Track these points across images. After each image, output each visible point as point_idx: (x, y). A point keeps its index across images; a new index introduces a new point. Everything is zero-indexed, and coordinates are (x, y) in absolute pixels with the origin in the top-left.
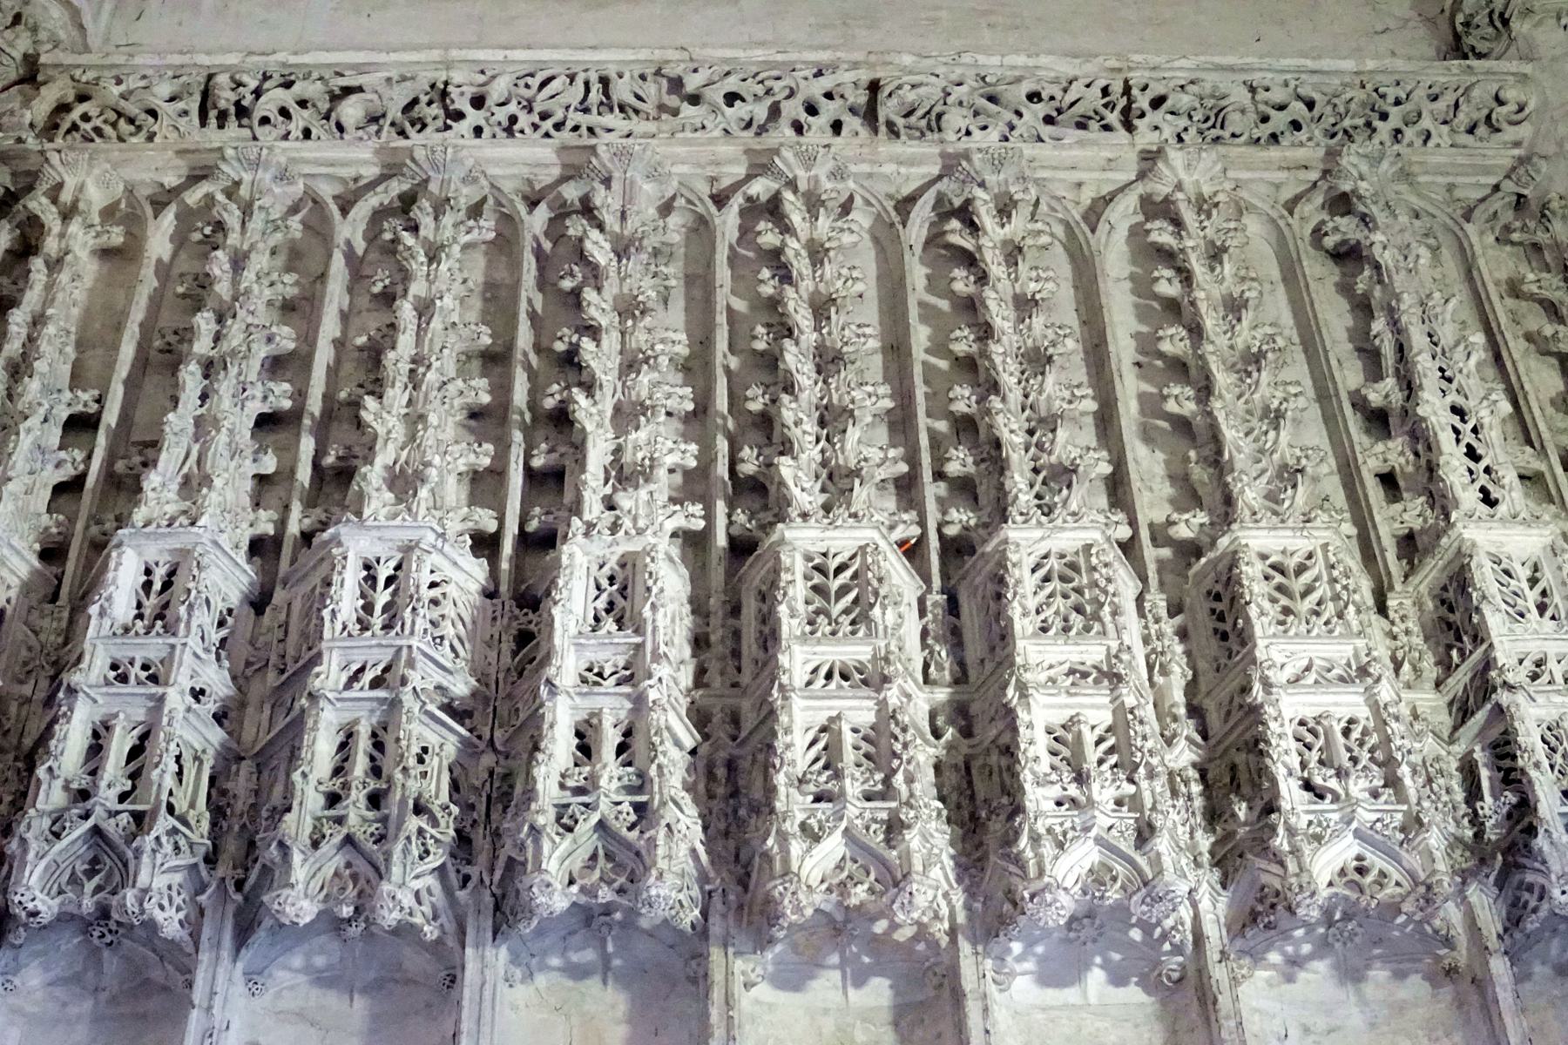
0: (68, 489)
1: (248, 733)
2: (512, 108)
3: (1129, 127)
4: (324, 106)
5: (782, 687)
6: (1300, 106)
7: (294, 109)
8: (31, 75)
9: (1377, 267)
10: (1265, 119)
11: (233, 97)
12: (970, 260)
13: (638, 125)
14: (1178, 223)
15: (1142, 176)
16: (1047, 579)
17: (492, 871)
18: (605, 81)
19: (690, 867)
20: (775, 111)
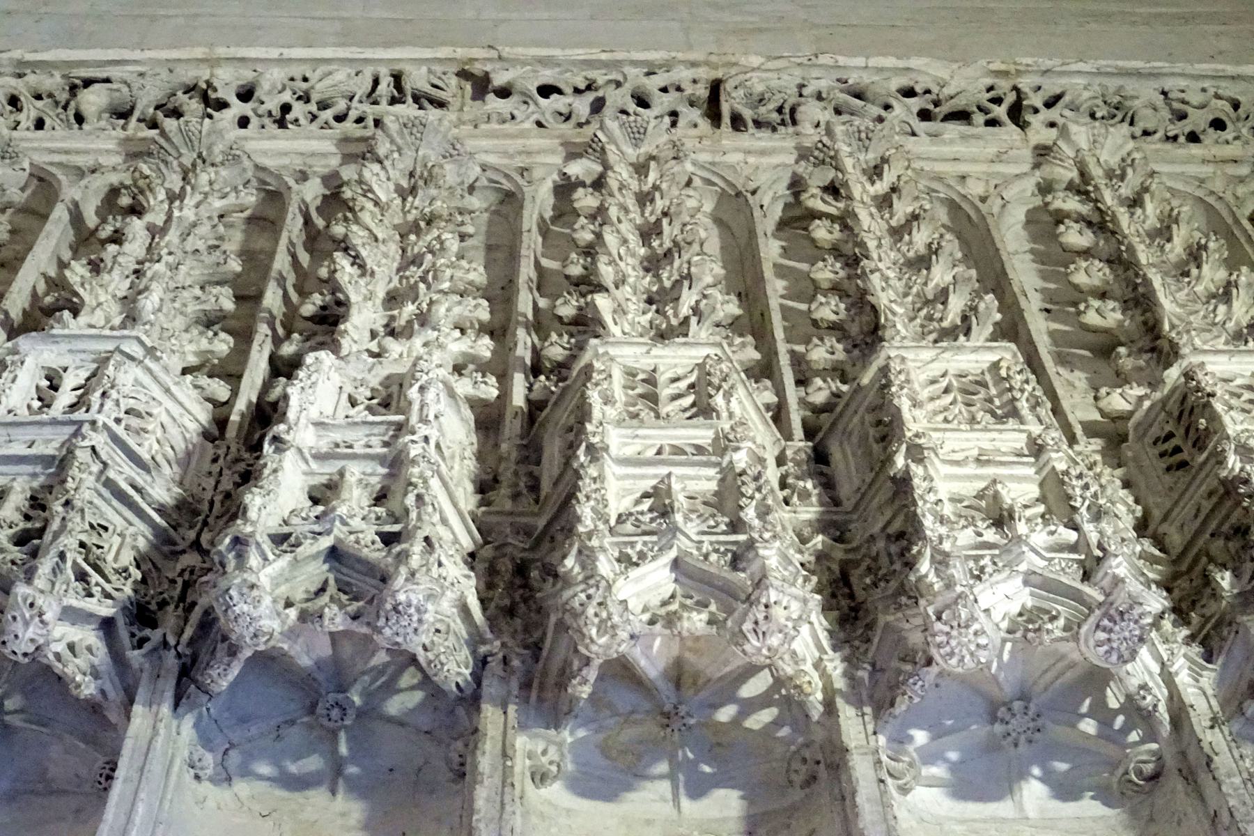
2: (287, 97)
3: (1023, 125)
4: (63, 97)
5: (591, 448)
7: (26, 99)
10: (1182, 116)
15: (1037, 166)
16: (947, 391)
17: (180, 633)
18: (397, 78)
19: (459, 627)
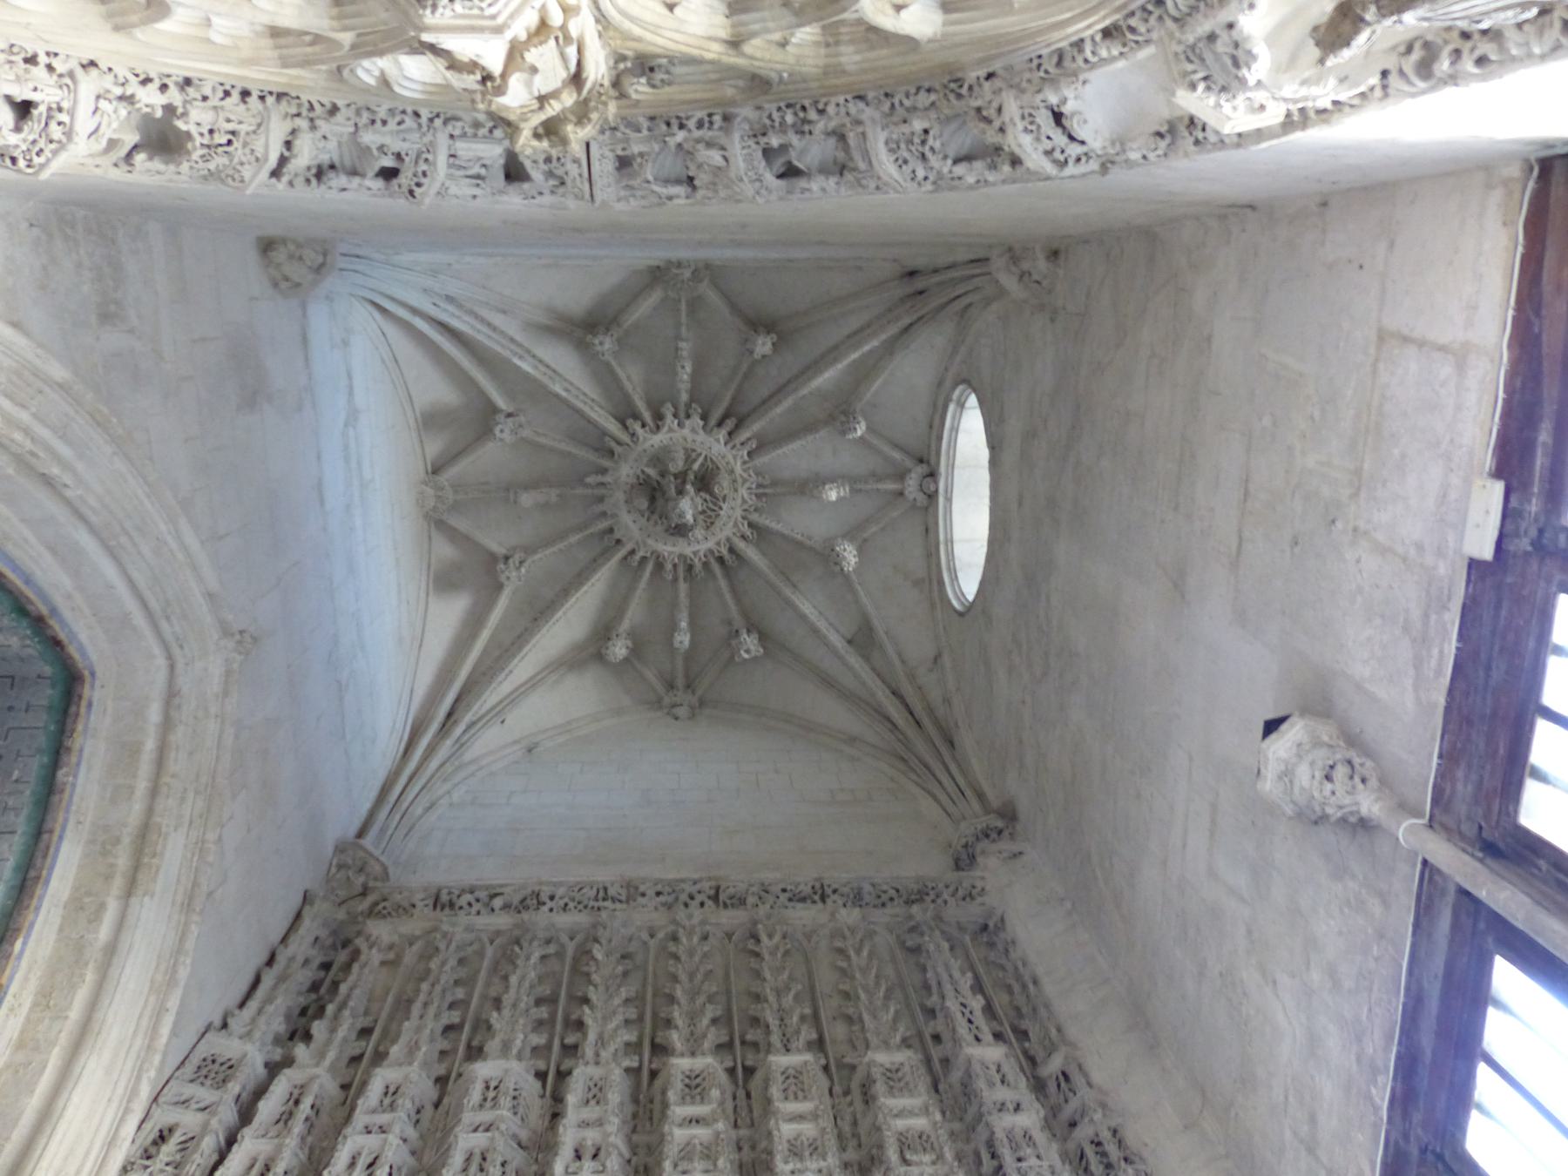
0: (356, 1060)
1: (425, 1159)
2: (566, 900)
4: (486, 900)
6: (892, 893)
8: (364, 893)
9: (928, 952)
11: (448, 898)
12: (757, 955)
13: (618, 906)
14: (844, 938)
20: (677, 899)
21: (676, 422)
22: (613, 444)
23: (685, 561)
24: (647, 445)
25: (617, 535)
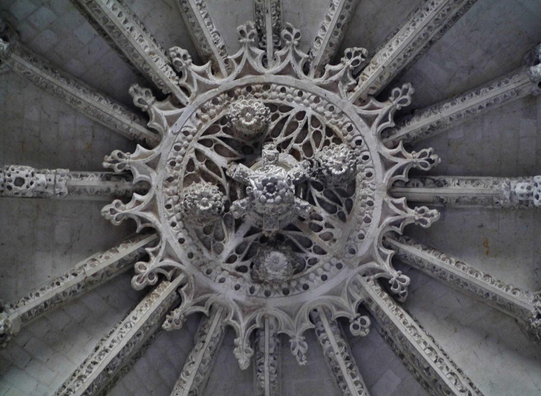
21: (137, 196)
22: (177, 314)
23: (406, 185)
24: (179, 250)
25: (351, 312)
